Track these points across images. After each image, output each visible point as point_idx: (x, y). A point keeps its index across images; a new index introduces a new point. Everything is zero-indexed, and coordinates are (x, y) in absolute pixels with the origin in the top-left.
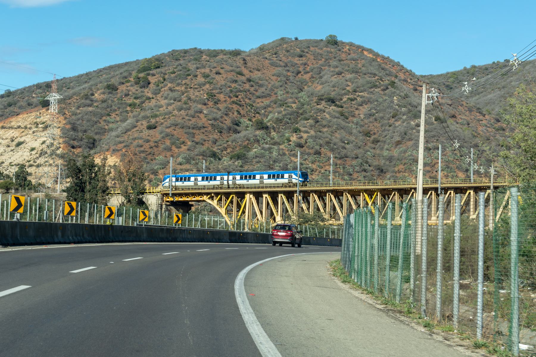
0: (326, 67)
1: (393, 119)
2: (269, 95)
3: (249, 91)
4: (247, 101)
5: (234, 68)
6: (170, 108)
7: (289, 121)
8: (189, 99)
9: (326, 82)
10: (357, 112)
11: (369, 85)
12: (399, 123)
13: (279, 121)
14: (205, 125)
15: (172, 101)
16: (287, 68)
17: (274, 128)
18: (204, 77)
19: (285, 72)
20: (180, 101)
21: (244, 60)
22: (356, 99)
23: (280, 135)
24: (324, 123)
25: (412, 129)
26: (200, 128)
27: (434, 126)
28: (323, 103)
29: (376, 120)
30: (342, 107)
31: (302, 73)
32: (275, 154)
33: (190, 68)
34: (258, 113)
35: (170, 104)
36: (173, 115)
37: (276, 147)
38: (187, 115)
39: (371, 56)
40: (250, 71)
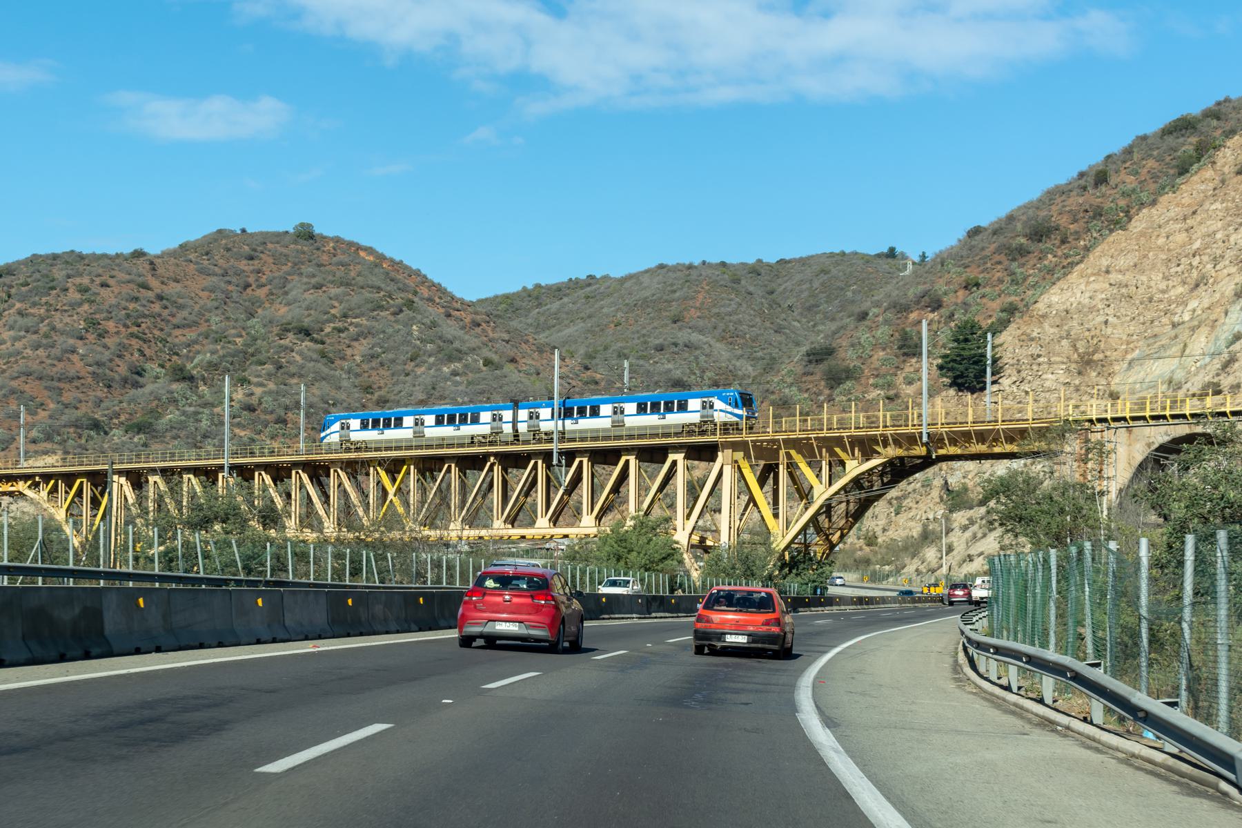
0: (296, 278)
1: (413, 364)
2: (196, 323)
3: (160, 315)
4: (157, 333)
5: (132, 277)
6: (18, 345)
7: (231, 368)
8: (54, 329)
9: (295, 301)
10: (349, 352)
11: (370, 306)
12: (423, 369)
13: (212, 366)
14: (80, 375)
15: (22, 333)
16: (228, 278)
17: (203, 379)
18: (80, 291)
19: (223, 285)
20: (36, 332)
21: (152, 263)
22: (347, 329)
23: (214, 389)
24: (293, 369)
25: (446, 379)
26: (71, 380)
27: (482, 375)
28: (291, 335)
29: (382, 364)
30: (323, 343)
31: (254, 287)
32: (205, 424)
33: (56, 276)
34: (177, 354)
35: (16, 339)
36: (23, 358)
37: (206, 411)
38: (48, 357)
39: (371, 258)
40: (163, 283)
